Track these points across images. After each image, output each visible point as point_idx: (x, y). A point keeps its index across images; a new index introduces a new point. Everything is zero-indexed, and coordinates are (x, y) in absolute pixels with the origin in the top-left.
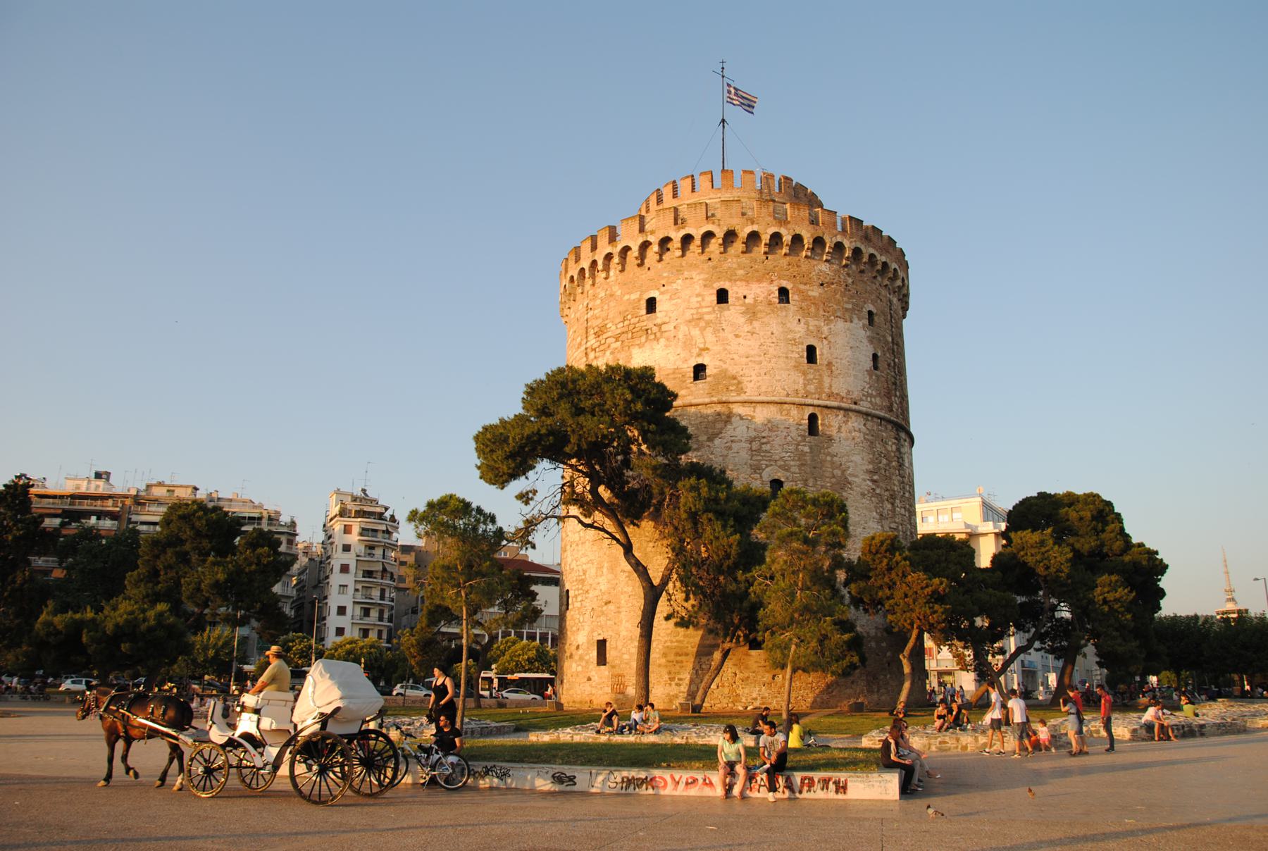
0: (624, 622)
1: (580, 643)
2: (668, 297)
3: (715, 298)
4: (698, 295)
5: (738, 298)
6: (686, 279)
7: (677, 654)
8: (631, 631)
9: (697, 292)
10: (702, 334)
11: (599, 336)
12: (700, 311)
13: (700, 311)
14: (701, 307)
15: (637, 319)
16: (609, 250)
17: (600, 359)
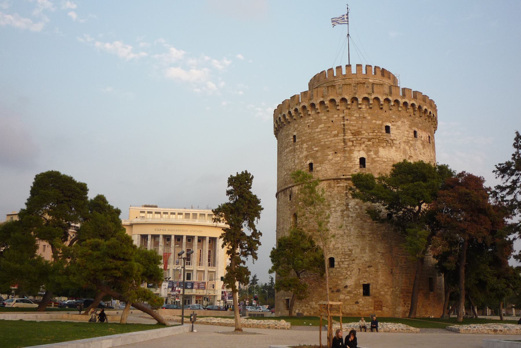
0: (380, 277)
1: (348, 285)
2: (396, 128)
3: (413, 134)
4: (407, 131)
5: (420, 137)
6: (403, 122)
7: (407, 293)
8: (385, 281)
9: (407, 129)
10: (409, 149)
11: (355, 135)
12: (408, 138)
13: (408, 138)
14: (409, 137)
15: (381, 134)
16: (366, 96)
17: (357, 147)
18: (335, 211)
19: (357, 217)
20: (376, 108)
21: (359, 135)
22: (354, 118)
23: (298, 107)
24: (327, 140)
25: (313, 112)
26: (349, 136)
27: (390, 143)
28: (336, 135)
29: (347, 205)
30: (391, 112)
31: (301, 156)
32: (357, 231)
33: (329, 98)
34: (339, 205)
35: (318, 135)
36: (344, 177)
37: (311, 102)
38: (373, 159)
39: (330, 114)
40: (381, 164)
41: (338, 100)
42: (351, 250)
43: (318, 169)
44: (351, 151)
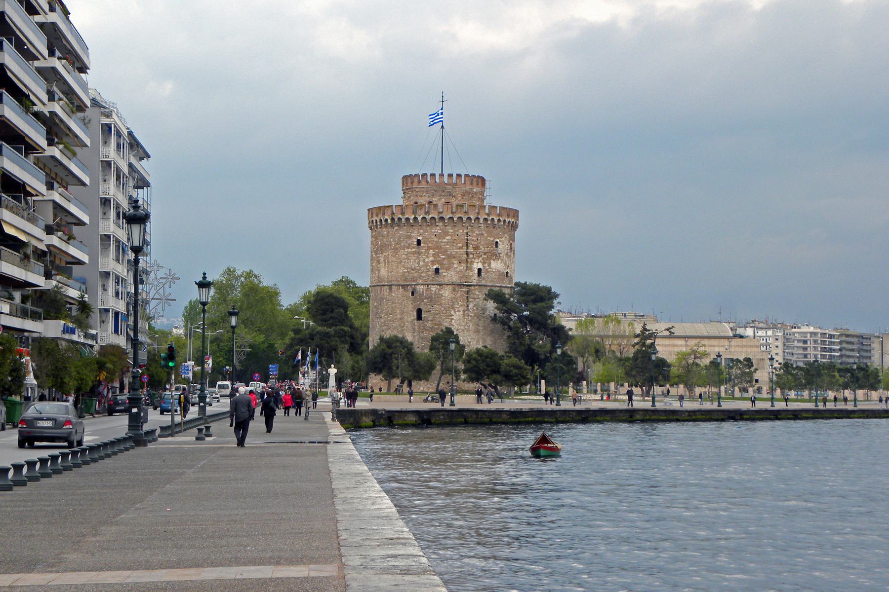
16: (486, 217)
18: (459, 311)
19: (475, 316)
20: (491, 226)
21: (478, 249)
22: (475, 235)
23: (427, 217)
24: (454, 251)
25: (441, 224)
26: (471, 250)
27: (497, 256)
28: (461, 248)
29: (468, 306)
30: (499, 230)
31: (426, 260)
32: (474, 328)
33: (458, 216)
34: (461, 306)
35: (445, 245)
36: (466, 284)
37: (442, 215)
38: (487, 269)
39: (456, 229)
40: (492, 274)
41: (464, 219)
42: (469, 342)
43: (444, 274)
44: (472, 263)
